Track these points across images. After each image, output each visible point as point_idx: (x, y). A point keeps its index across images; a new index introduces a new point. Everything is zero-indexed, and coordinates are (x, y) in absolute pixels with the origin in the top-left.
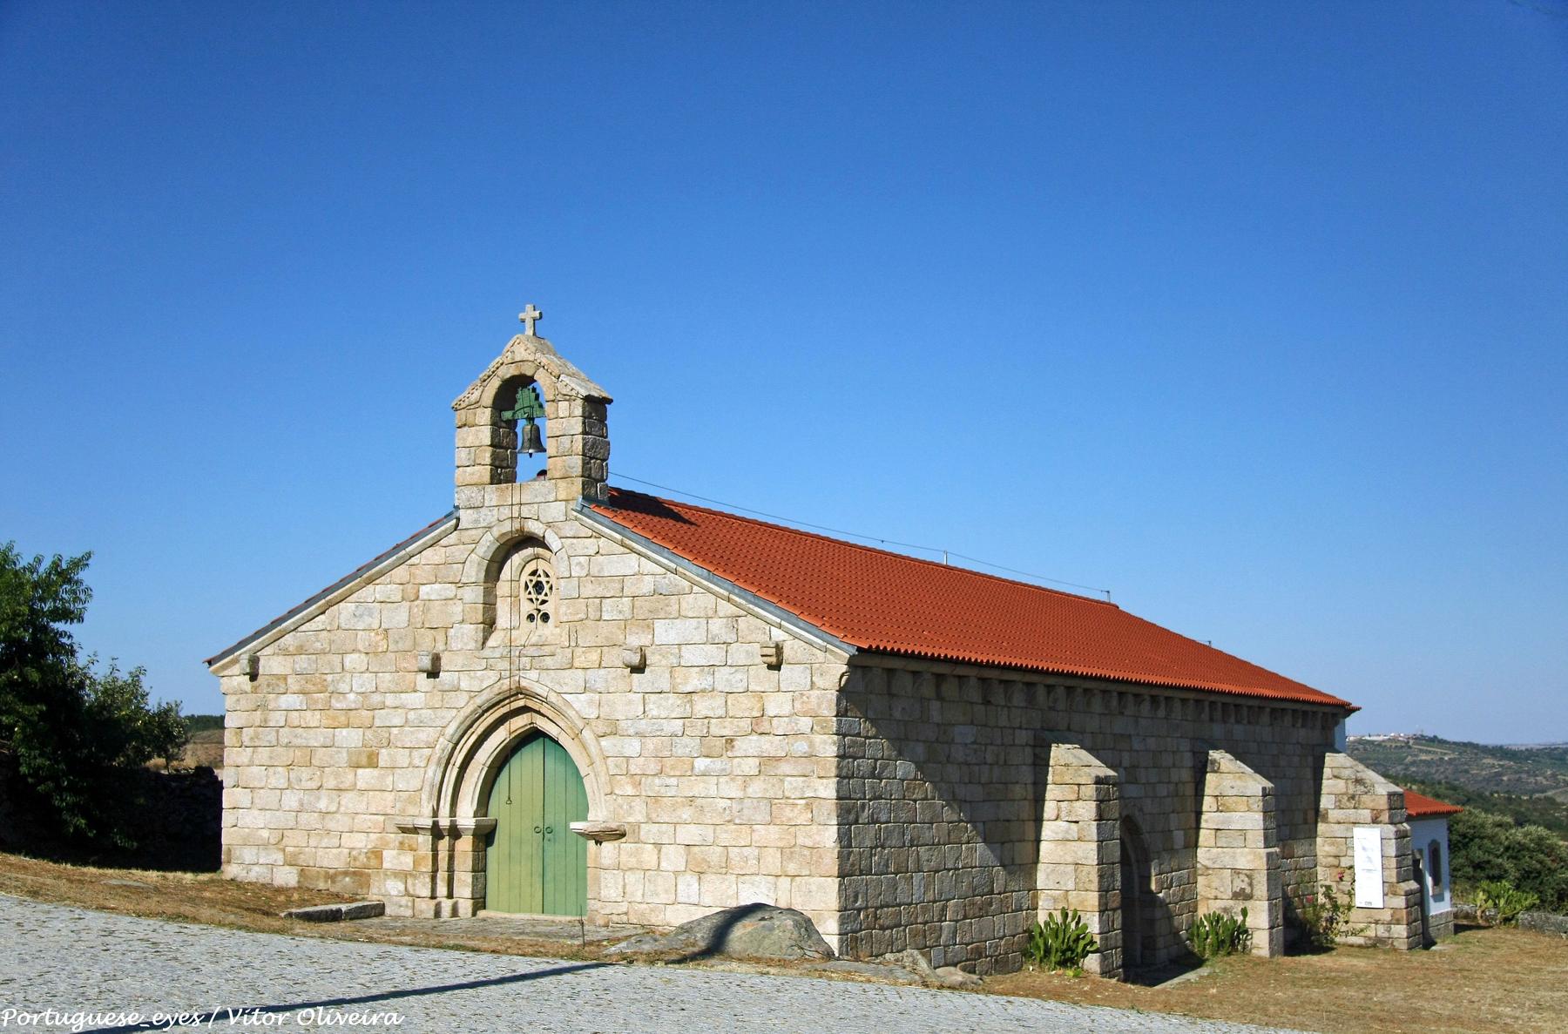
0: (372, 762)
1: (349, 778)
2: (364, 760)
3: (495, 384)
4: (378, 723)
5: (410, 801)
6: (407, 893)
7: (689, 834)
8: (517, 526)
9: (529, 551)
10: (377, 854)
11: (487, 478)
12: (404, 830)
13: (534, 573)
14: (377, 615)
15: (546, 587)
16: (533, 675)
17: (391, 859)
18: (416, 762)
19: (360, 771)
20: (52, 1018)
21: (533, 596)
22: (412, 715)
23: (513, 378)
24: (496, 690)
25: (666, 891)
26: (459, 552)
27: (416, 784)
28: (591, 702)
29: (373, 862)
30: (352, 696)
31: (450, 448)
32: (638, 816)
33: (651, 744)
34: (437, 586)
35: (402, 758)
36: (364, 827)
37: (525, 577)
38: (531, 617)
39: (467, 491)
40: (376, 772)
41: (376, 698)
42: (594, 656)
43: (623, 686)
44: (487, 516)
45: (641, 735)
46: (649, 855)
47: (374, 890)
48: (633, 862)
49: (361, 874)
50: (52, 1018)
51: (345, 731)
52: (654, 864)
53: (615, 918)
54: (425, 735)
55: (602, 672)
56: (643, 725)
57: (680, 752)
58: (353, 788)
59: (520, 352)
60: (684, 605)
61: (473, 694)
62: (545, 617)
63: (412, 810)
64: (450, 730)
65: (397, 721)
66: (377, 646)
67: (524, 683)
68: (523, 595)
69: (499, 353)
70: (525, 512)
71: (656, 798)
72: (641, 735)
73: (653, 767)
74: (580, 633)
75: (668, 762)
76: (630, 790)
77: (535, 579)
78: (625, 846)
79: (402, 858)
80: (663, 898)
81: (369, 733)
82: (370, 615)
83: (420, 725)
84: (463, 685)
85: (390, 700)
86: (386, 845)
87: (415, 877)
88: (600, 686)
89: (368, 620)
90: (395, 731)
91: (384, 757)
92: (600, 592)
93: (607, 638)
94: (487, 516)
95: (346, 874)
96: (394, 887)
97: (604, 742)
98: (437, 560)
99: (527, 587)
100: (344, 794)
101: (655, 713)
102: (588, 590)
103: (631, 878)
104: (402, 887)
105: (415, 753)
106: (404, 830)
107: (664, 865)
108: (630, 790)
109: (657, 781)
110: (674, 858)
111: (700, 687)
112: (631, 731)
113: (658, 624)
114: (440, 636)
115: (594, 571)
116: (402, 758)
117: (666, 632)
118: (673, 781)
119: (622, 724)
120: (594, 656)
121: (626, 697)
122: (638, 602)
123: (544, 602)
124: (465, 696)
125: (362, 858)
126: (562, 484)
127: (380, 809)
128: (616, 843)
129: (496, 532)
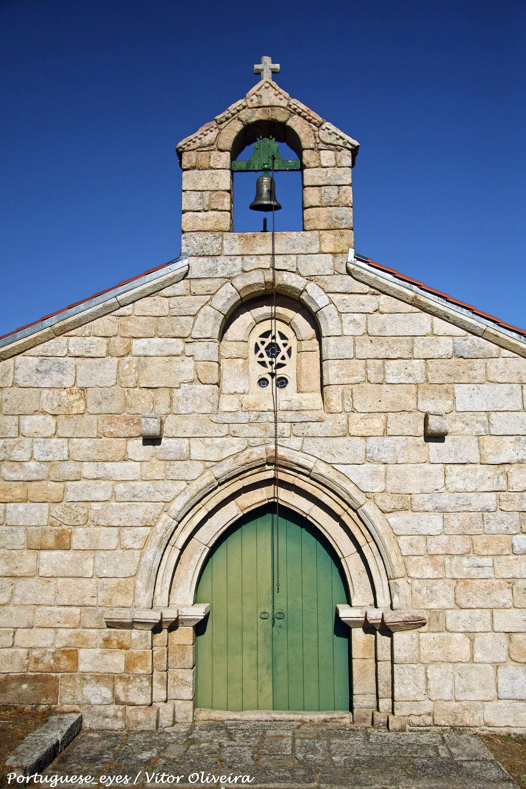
0: (62, 543)
1: (28, 561)
2: (51, 541)
3: (238, 127)
4: (70, 496)
5: (119, 589)
6: (117, 701)
7: (506, 620)
8: (269, 277)
9: (266, 310)
10: (71, 654)
11: (226, 224)
12: (111, 625)
13: (266, 335)
14: (70, 370)
15: (284, 351)
16: (296, 443)
17: (88, 660)
18: (128, 542)
19: (44, 554)
20: (38, 778)
21: (267, 359)
22: (121, 488)
23: (259, 123)
24: (242, 459)
25: (483, 686)
26: (190, 304)
27: (128, 568)
28: (374, 474)
29: (64, 664)
30: (32, 465)
31: (179, 191)
32: (443, 600)
33: (455, 521)
34: (157, 340)
35: (107, 538)
36: (52, 621)
37: (255, 338)
38: (263, 382)
39: (200, 238)
40: (68, 555)
41: (69, 468)
42: (377, 423)
43: (414, 455)
44: (225, 266)
45: (442, 511)
46: (459, 646)
47: (67, 699)
48: (437, 654)
49: (46, 680)
50: (38, 778)
51: (21, 507)
52: (465, 654)
53: (415, 720)
54: (139, 512)
55: (388, 440)
56: (444, 500)
57: (493, 529)
58: (35, 573)
59: (267, 97)
60: (492, 369)
61: (209, 464)
62: (282, 382)
63: (120, 600)
64: (178, 506)
65: (99, 495)
66: (70, 405)
67: (281, 452)
68: (254, 358)
69: (243, 96)
70: (279, 263)
71: (466, 581)
72: (442, 511)
73: (460, 545)
74: (358, 397)
75: (479, 541)
76: (429, 572)
77: (268, 341)
78: (425, 636)
79: (108, 658)
80: (479, 694)
81: (57, 509)
82: (61, 371)
83: (134, 499)
84: (195, 454)
85: (88, 470)
86: (85, 643)
87: (128, 680)
88: (386, 456)
89: (57, 377)
90: (96, 506)
91: (80, 537)
92: (382, 352)
93: (393, 403)
94: (225, 266)
95: (22, 679)
96: (97, 694)
97: (392, 519)
98: (157, 311)
99: (257, 348)
100: (20, 582)
101: (460, 485)
102: (367, 350)
103: (434, 672)
104: (107, 693)
105: (126, 532)
106: (111, 625)
107: (478, 656)
108: (429, 572)
109: (465, 561)
110: (491, 648)
111: (515, 459)
112: (429, 506)
113: (459, 390)
114: (163, 397)
115: (374, 330)
116: (107, 538)
117: (466, 397)
118: (488, 561)
119: (417, 499)
120: (377, 423)
121: (420, 470)
122: (432, 365)
123: (280, 366)
124: (200, 466)
125: (49, 660)
126: (328, 236)
127: (75, 600)
128: (413, 633)
129: (240, 283)
